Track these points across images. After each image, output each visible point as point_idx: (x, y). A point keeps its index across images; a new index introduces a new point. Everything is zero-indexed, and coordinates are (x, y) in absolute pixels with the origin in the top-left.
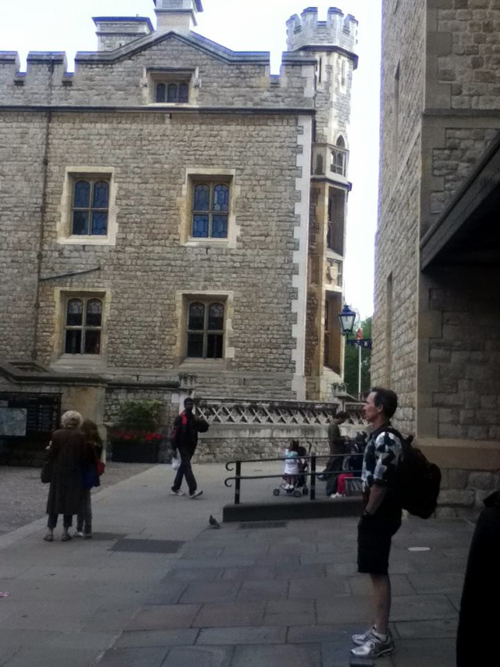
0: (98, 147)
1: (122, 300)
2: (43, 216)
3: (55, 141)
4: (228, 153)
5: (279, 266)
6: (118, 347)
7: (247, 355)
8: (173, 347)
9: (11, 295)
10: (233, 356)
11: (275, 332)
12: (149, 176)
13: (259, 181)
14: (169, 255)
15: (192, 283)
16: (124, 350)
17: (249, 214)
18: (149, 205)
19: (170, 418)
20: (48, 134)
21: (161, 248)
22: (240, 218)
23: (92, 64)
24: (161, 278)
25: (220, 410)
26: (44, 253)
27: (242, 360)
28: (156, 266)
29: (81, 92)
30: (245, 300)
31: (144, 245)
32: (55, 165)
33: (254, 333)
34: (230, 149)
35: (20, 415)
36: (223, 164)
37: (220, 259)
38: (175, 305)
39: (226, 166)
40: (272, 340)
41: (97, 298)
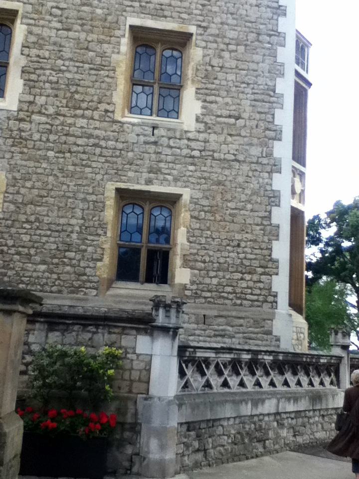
1: (23, 191)
6: (12, 260)
7: (207, 281)
8: (99, 264)
10: (188, 282)
12: (73, 21)
13: (228, 44)
14: (97, 132)
15: (131, 174)
16: (21, 264)
17: (214, 86)
18: (71, 59)
19: (132, 381)
21: (85, 121)
22: (201, 91)
24: (84, 162)
27: (201, 286)
28: (78, 145)
30: (205, 202)
31: (60, 115)
33: (218, 250)
36: (179, 17)
37: (172, 144)
38: (103, 202)
39: (183, 21)
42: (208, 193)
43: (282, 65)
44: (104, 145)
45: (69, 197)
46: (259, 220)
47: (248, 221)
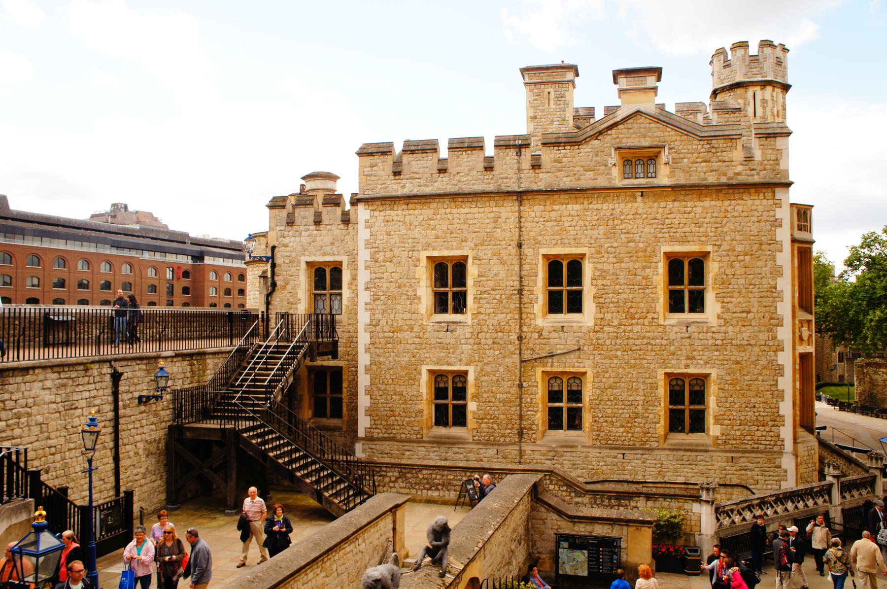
0: (571, 228)
1: (603, 380)
2: (520, 298)
3: (527, 224)
4: (703, 229)
5: (763, 343)
7: (733, 432)
8: (658, 425)
9: (495, 376)
11: (762, 410)
14: (648, 335)
15: (674, 362)
17: (729, 290)
18: (625, 284)
20: (520, 218)
22: (720, 295)
23: (559, 146)
24: (641, 357)
25: (736, 512)
26: (523, 335)
27: (728, 437)
29: (549, 174)
30: (728, 378)
32: (529, 248)
34: (705, 225)
35: (581, 556)
39: (703, 243)
40: (759, 418)
41: (578, 377)
42: (729, 371)
43: (781, 267)
44: (654, 343)
45: (634, 382)
46: (767, 387)
47: (760, 389)
